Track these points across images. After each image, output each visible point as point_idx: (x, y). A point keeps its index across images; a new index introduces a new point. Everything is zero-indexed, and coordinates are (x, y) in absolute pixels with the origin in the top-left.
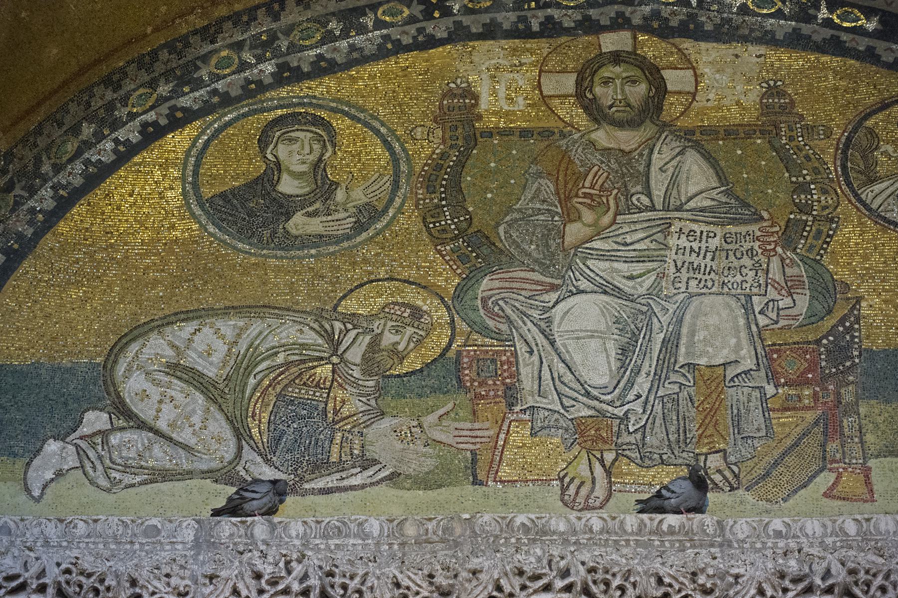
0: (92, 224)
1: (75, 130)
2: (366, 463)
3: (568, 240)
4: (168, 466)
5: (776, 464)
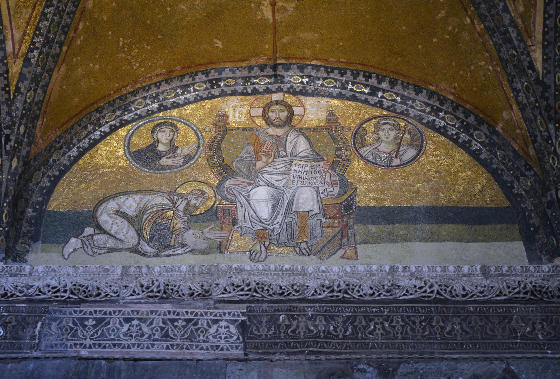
1: (86, 127)
2: (183, 245)
3: (257, 167)
4: (114, 247)
5: (324, 246)
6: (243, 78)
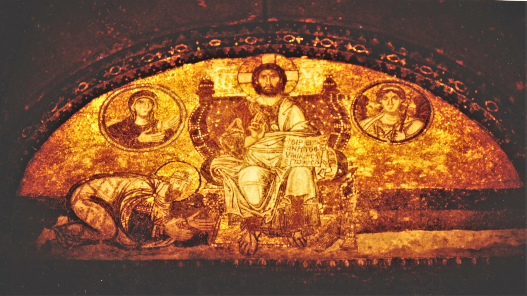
0: (63, 138)
3: (247, 144)
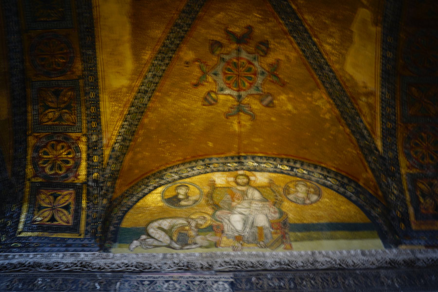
1: (140, 187)
2: (195, 244)
6: (223, 163)
